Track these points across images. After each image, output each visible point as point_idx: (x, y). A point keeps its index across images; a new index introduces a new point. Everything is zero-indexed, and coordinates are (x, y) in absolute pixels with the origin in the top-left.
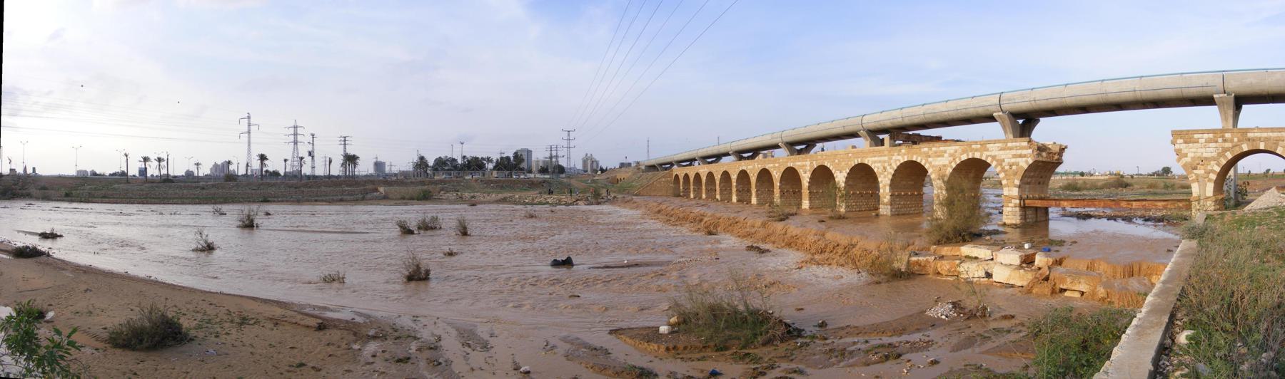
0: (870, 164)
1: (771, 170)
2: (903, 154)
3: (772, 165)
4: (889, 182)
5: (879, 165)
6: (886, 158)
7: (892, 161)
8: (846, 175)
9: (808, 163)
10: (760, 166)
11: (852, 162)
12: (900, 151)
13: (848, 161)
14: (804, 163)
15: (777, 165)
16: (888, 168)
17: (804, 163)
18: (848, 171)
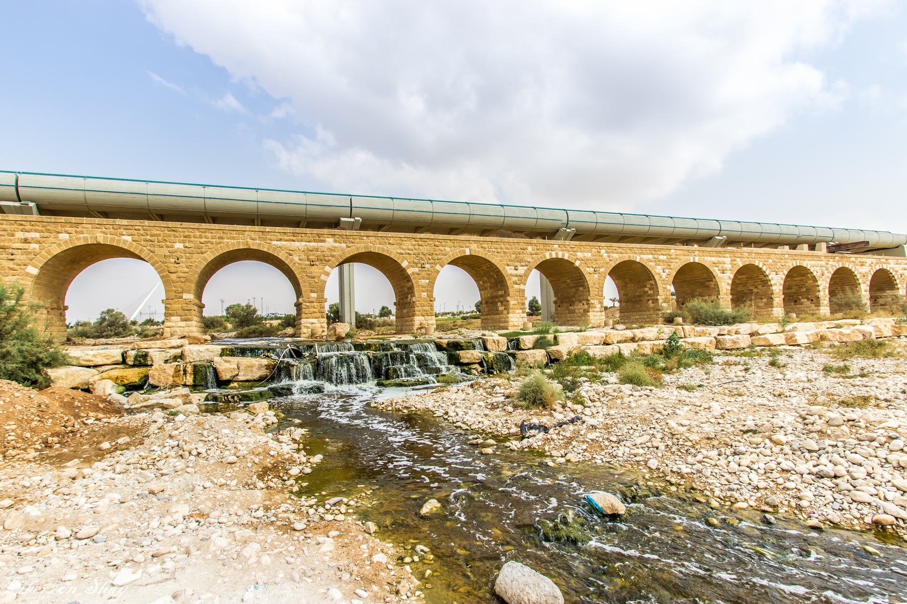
0: (808, 268)
1: (650, 265)
2: (836, 262)
3: (650, 257)
4: (828, 285)
5: (818, 268)
6: (823, 263)
7: (829, 266)
8: (784, 277)
9: (728, 260)
10: (615, 256)
11: (791, 264)
12: (834, 258)
13: (786, 262)
14: (721, 259)
16: (826, 272)
17: (721, 259)
18: (786, 273)
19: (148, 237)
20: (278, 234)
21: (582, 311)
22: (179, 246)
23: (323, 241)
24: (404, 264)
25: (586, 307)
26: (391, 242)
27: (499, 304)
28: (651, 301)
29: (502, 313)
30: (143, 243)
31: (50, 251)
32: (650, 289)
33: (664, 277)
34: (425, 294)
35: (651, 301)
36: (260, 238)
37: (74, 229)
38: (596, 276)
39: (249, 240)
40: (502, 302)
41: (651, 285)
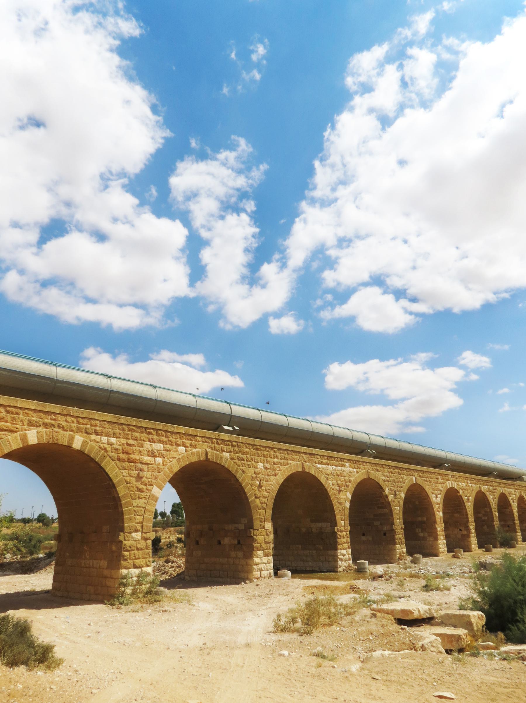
10: (474, 485)
15: (491, 488)
19: (241, 455)
20: (319, 457)
21: (460, 537)
22: (261, 466)
23: (344, 466)
24: (387, 491)
25: (465, 532)
26: (378, 468)
27: (418, 530)
28: (486, 527)
29: (424, 538)
30: (237, 461)
31: (172, 468)
32: (484, 515)
33: (494, 504)
34: (398, 521)
35: (486, 527)
36: (309, 460)
37: (189, 442)
38: (469, 503)
39: (303, 462)
40: (424, 530)
41: (486, 512)
